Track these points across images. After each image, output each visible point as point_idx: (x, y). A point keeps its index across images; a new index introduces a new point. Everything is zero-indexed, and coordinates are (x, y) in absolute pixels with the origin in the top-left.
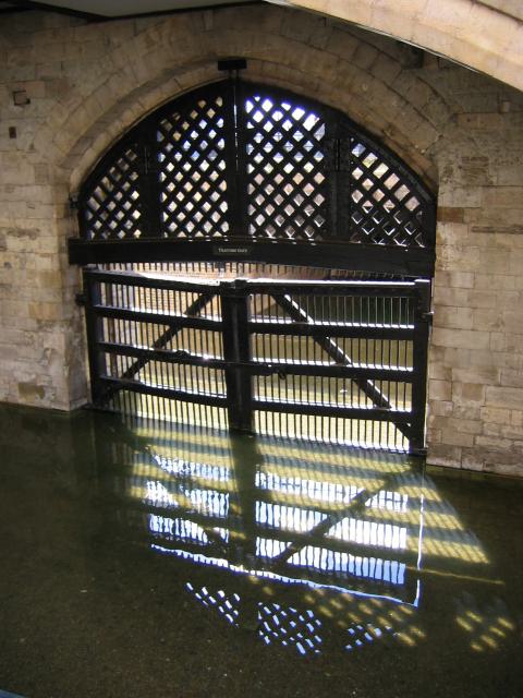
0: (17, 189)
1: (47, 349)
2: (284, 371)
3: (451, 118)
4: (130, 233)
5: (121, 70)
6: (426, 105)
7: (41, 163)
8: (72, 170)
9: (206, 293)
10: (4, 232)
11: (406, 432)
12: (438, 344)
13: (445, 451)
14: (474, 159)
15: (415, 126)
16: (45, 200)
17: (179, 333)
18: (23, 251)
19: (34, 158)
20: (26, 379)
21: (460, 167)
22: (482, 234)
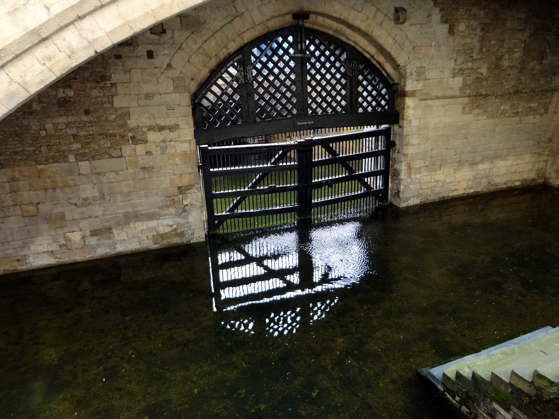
0: (157, 97)
1: (187, 205)
2: (330, 183)
3: (413, 48)
5: (242, 14)
6: (404, 42)
7: (178, 77)
10: (145, 129)
12: (405, 153)
13: (408, 199)
14: (421, 67)
16: (183, 103)
17: (269, 175)
18: (164, 141)
19: (170, 73)
21: (415, 71)
22: (423, 101)
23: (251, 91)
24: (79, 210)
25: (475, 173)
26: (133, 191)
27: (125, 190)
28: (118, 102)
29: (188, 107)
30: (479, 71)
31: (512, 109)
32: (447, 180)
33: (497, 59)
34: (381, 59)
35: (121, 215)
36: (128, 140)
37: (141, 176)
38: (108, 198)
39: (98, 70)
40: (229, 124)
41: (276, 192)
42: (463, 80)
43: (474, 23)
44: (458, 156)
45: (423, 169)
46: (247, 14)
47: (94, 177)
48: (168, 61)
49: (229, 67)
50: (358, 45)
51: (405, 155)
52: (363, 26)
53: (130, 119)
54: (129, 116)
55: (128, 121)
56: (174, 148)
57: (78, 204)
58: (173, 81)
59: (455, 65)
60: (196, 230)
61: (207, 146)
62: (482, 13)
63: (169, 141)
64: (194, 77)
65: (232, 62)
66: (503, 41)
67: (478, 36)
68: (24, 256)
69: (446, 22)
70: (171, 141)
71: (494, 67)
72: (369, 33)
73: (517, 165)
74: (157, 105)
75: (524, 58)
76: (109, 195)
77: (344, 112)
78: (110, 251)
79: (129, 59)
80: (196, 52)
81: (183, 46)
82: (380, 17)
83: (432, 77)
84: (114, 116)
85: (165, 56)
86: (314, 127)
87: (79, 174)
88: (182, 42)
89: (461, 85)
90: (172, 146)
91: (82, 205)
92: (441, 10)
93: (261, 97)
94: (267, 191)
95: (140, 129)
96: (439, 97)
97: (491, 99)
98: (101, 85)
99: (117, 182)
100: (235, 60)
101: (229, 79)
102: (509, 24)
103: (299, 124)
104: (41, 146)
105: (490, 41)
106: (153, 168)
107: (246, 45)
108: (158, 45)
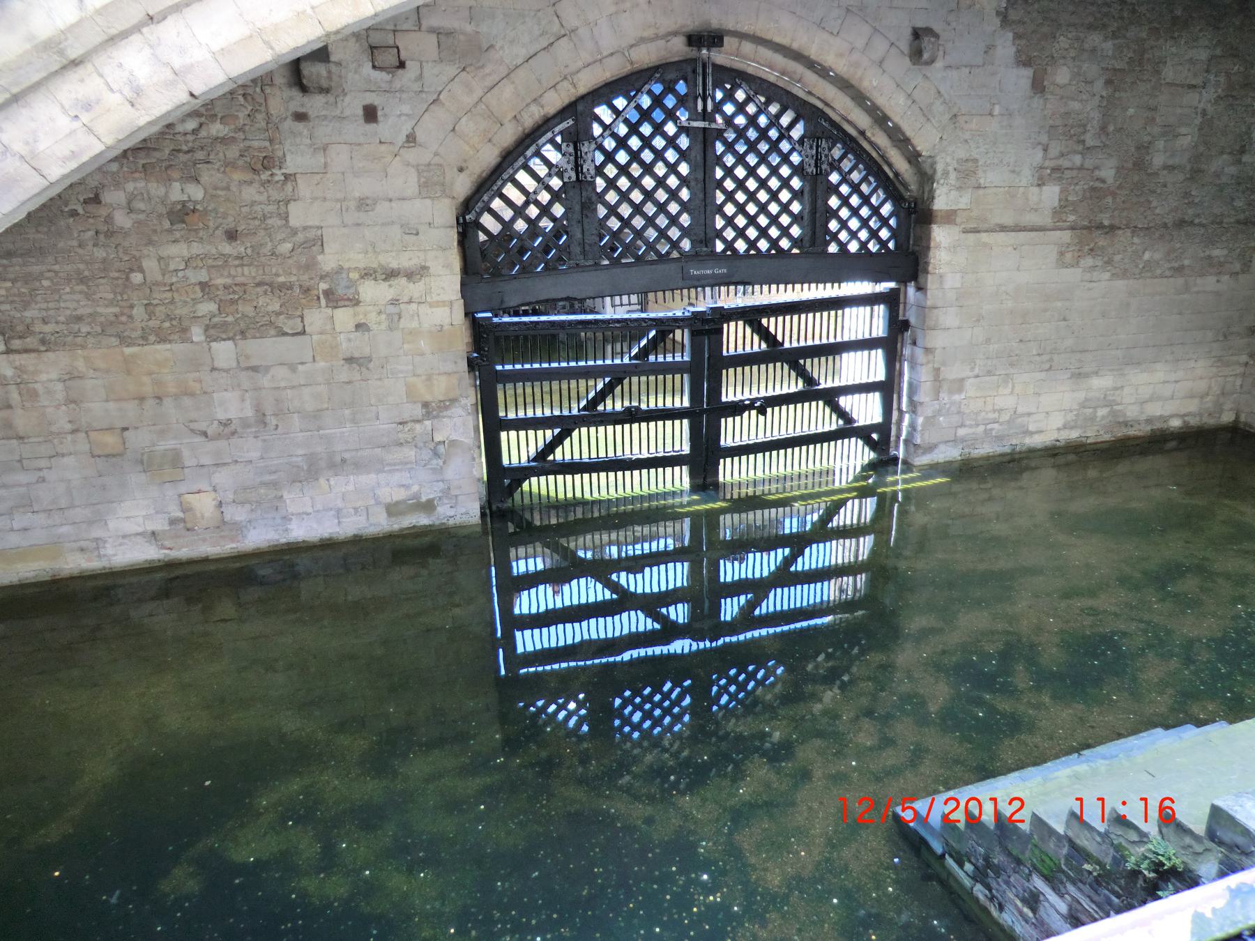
0: (382, 208)
6: (931, 104)
7: (429, 164)
9: (665, 327)
10: (354, 276)
12: (929, 346)
16: (439, 221)
17: (626, 382)
18: (395, 302)
19: (411, 155)
20: (399, 495)
23: (590, 199)
24: (211, 446)
25: (1081, 395)
26: (327, 409)
27: (310, 406)
28: (298, 215)
30: (1097, 173)
31: (1169, 261)
32: (1020, 410)
33: (1138, 148)
34: (881, 140)
35: (300, 459)
36: (319, 298)
37: (344, 377)
38: (274, 422)
39: (256, 144)
40: (539, 269)
41: (639, 421)
42: (1061, 192)
43: (1091, 68)
44: (1045, 357)
45: (968, 383)
46: (583, 31)
47: (243, 376)
48: (410, 130)
49: (544, 145)
50: (831, 107)
51: (928, 350)
52: (840, 66)
53: (323, 252)
54: (322, 245)
55: (320, 258)
56: (416, 318)
57: (209, 432)
59: (1045, 158)
61: (489, 315)
62: (1109, 45)
64: (464, 165)
65: (549, 135)
66: (1155, 109)
67: (1097, 98)
68: (97, 540)
69: (1026, 63)
70: (410, 302)
71: (1130, 165)
72: (853, 82)
73: (1176, 382)
74: (383, 224)
75: (1201, 149)
76: (276, 415)
77: (795, 251)
78: (277, 537)
79: (324, 123)
81: (441, 97)
82: (880, 46)
83: (991, 182)
84: (289, 246)
85: (403, 118)
86: (727, 281)
87: (213, 369)
88: (440, 89)
89: (1056, 204)
91: (218, 436)
92: (1017, 36)
93: (613, 211)
94: (620, 417)
95: (344, 275)
96: (1006, 227)
97: (1123, 236)
98: (265, 176)
99: (293, 387)
100: (557, 129)
101: (542, 171)
102: (1169, 73)
104: (132, 307)
105: (1125, 109)
106: (370, 359)
107: (583, 97)
108: (388, 95)
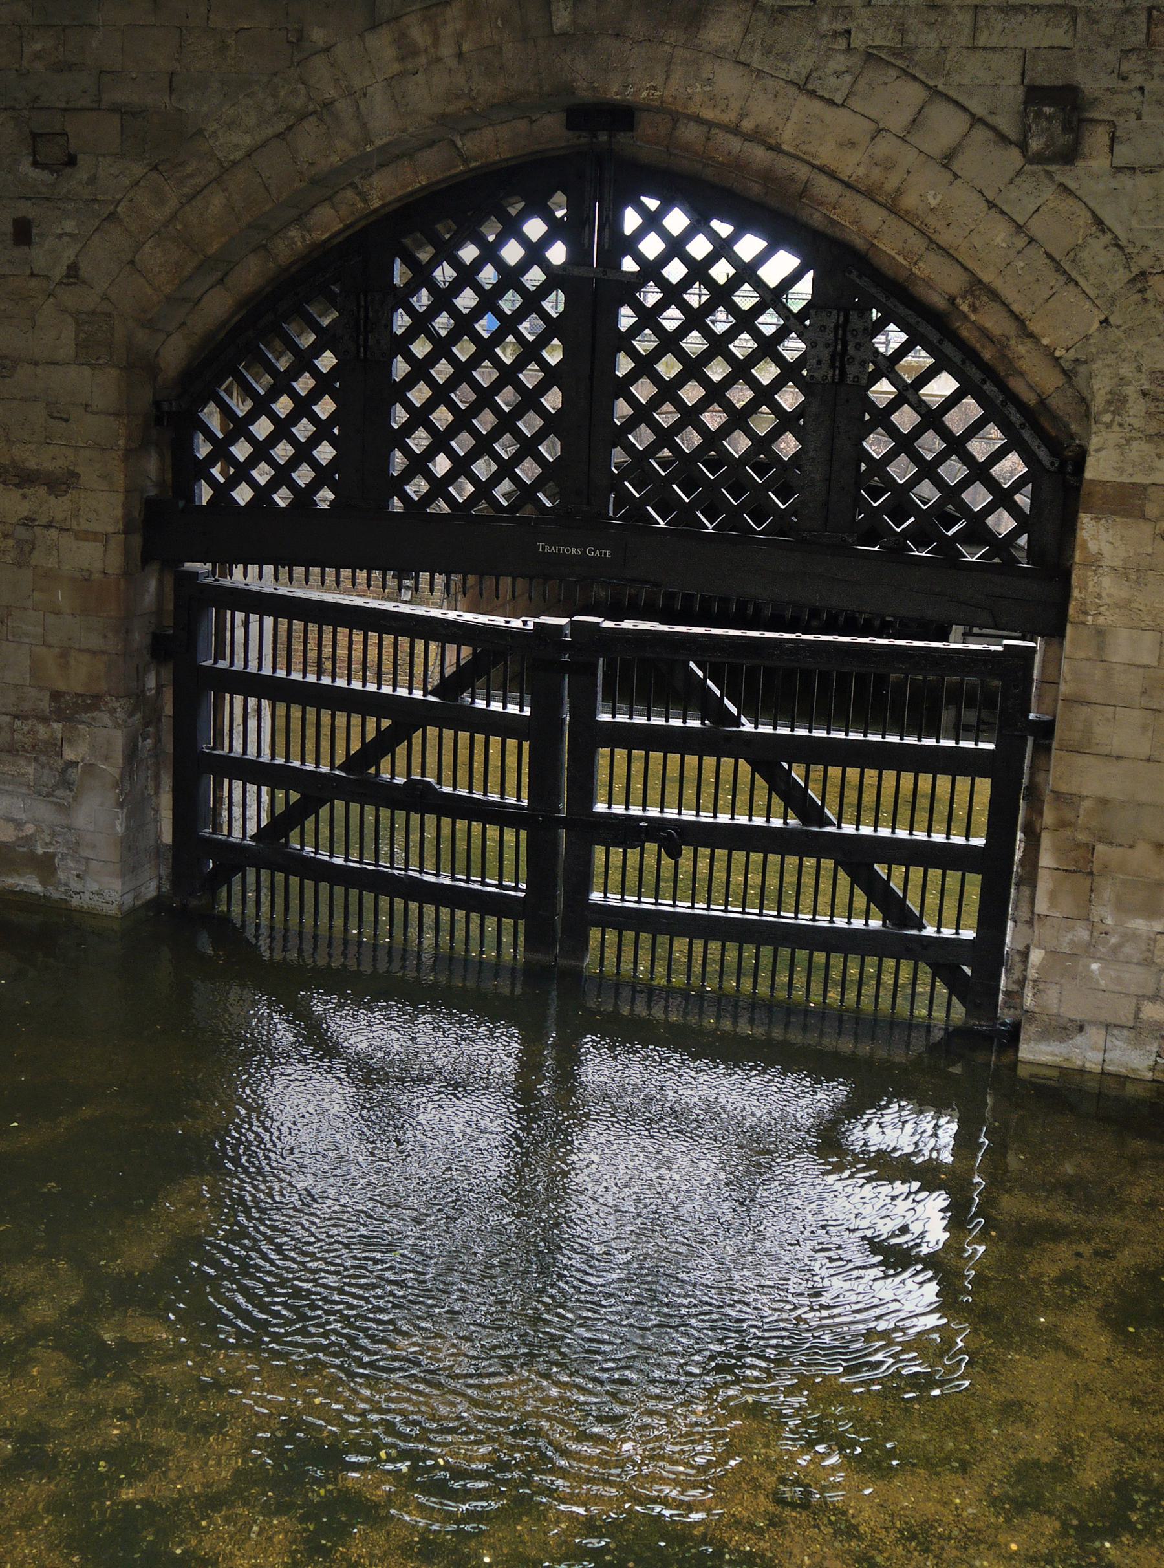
3: (1132, 281)
4: (304, 496)
7: (93, 313)
8: (169, 335)
11: (958, 986)
12: (1063, 788)
15: (1047, 293)
18: (28, 522)
21: (1144, 394)
29: (112, 418)
46: (343, 107)
48: (73, 258)
58: (77, 324)
60: (94, 865)
63: (44, 526)
70: (49, 525)
74: (22, 399)
80: (158, 233)
81: (119, 209)
85: (66, 239)
90: (49, 543)
103: (547, 549)
